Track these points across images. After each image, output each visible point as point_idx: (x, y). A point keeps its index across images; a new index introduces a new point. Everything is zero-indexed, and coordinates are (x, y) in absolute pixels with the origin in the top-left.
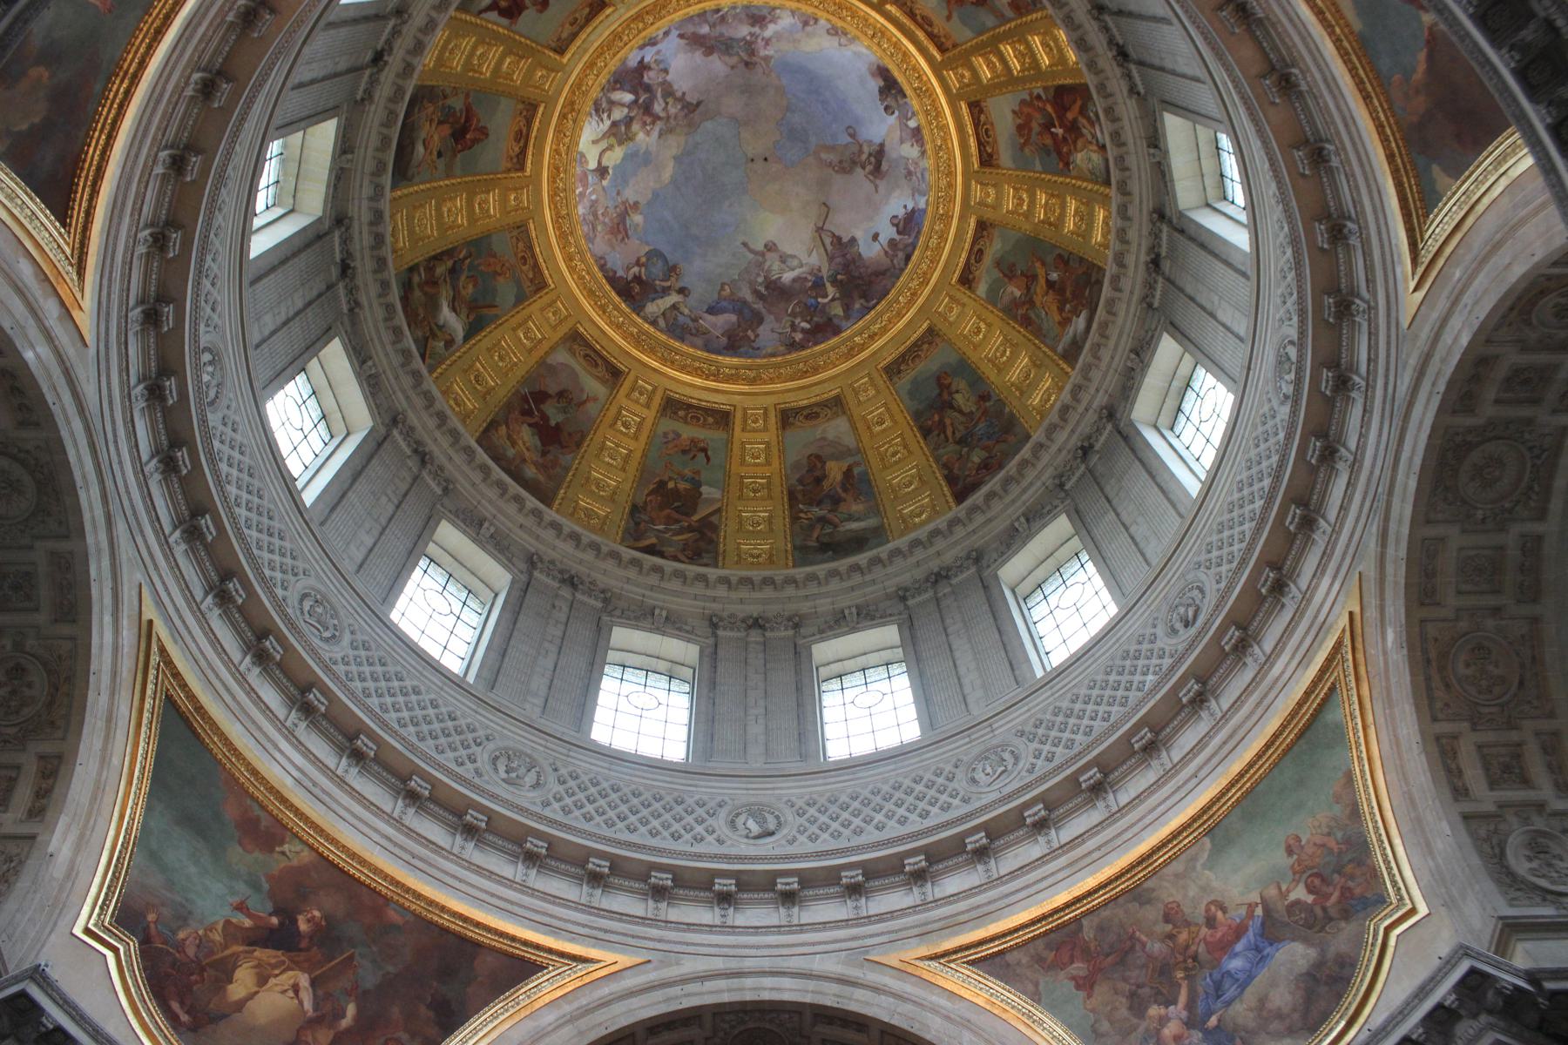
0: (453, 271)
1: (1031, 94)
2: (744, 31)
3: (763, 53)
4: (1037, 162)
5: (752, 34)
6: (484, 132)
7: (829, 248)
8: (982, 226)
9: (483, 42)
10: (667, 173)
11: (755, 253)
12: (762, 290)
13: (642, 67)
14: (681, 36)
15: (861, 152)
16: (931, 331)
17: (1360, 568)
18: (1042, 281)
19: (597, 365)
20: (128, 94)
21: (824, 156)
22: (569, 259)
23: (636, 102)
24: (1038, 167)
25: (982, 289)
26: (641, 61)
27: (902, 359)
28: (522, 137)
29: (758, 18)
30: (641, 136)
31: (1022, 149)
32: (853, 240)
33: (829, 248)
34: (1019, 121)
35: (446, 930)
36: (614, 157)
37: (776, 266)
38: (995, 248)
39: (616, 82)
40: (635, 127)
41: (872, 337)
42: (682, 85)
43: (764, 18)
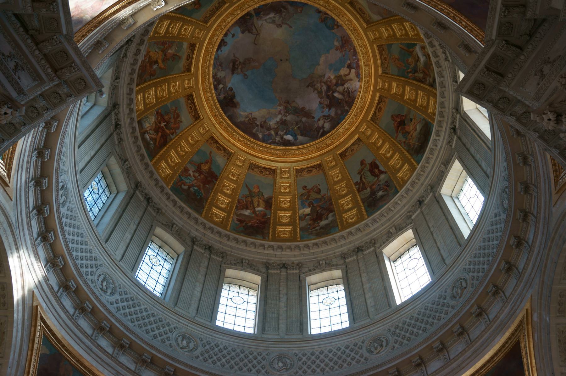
0: (416, 71)
1: (176, 133)
2: (289, 118)
3: (281, 108)
4: (169, 106)
5: (286, 116)
6: (393, 118)
7: (253, 28)
8: (189, 70)
9: (387, 158)
10: (322, 59)
11: (286, 24)
12: (283, 10)
13: (329, 107)
14: (313, 118)
15: (241, 69)
16: (206, 22)
17: (13, 202)
18: (160, 61)
19: (360, 9)
20: (481, 368)
21: (257, 64)
22: (367, 53)
23: (333, 92)
24: (169, 105)
25: (185, 45)
26: (330, 109)
27: (218, 9)
28: (378, 109)
29: (283, 123)
30: (332, 77)
31: (176, 108)
32: (243, 32)
33: (253, 28)
34: (179, 119)
35: (466, 17)
36: (344, 71)
37: (277, 19)
38: (182, 63)
39: (340, 103)
40: (334, 81)
41: (231, 14)
42: (314, 96)
43: (281, 124)
